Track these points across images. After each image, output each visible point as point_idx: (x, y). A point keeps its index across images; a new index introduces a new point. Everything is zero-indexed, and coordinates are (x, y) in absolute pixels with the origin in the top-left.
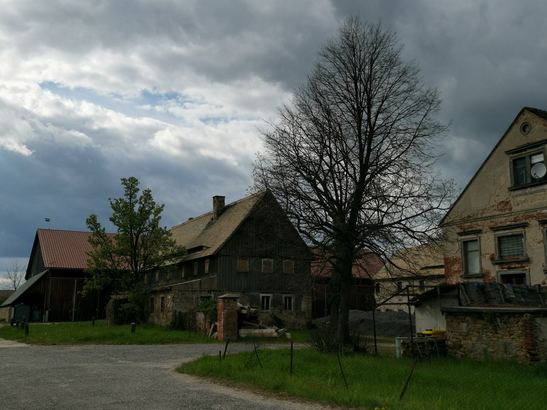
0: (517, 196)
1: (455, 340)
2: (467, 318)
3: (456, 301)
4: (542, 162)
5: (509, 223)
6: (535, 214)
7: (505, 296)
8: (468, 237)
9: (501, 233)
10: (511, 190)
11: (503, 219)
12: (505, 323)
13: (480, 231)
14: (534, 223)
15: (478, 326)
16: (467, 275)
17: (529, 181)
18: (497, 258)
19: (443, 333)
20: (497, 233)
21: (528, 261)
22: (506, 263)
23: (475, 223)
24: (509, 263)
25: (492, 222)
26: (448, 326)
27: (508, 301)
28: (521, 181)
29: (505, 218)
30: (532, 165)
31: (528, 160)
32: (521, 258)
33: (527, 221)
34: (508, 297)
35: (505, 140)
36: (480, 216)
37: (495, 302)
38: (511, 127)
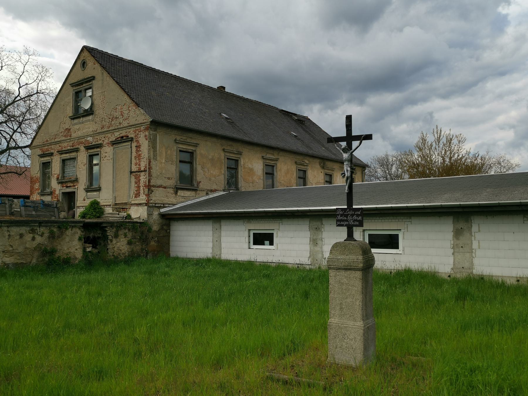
0: (76, 124)
5: (69, 148)
8: (45, 159)
9: (65, 156)
10: (73, 118)
11: (66, 144)
13: (52, 154)
14: (82, 148)
23: (50, 147)
24: (67, 182)
25: (60, 146)
29: (67, 144)
32: (73, 179)
33: (79, 147)
35: (72, 74)
36: (53, 141)
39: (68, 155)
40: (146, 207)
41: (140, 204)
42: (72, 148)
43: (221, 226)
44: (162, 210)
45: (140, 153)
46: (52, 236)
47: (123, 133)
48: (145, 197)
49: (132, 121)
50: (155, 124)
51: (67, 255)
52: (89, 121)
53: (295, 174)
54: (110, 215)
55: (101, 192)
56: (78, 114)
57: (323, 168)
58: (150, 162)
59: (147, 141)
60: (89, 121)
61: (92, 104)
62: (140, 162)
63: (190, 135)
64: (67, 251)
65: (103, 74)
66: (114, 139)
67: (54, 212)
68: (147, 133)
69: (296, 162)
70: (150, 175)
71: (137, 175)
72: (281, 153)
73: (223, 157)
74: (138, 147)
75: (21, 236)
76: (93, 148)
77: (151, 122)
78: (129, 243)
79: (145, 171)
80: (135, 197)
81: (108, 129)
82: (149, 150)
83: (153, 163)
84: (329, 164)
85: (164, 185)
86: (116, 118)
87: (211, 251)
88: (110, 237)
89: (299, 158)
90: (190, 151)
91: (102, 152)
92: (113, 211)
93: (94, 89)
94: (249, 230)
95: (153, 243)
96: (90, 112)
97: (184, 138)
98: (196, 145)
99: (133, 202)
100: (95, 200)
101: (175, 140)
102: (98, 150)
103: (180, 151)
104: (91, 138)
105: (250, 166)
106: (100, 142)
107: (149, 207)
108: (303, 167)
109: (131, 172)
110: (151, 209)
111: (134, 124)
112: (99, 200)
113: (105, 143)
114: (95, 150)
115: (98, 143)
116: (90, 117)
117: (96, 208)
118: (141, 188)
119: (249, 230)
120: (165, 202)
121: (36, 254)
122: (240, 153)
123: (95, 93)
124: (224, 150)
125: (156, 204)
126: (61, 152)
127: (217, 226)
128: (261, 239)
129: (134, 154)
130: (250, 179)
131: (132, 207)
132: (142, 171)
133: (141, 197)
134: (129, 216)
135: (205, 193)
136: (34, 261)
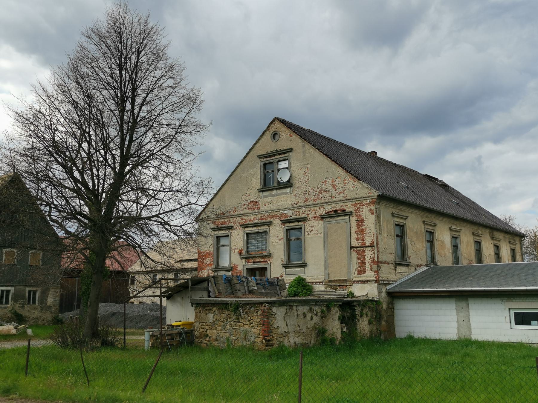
0: (265, 197)
1: (202, 330)
2: (214, 309)
3: (205, 293)
4: (286, 168)
5: (256, 221)
6: (278, 214)
7: (248, 288)
8: (220, 232)
9: (249, 230)
10: (260, 191)
11: (252, 217)
12: (246, 313)
13: (231, 228)
14: (277, 222)
15: (224, 316)
16: (218, 269)
17: (275, 184)
18: (244, 252)
19: (191, 324)
20: (246, 229)
21: (270, 256)
22: (252, 258)
23: (228, 219)
24: (254, 257)
25: (242, 219)
26: (196, 316)
27: (251, 292)
28: (269, 184)
29: (254, 217)
30: (279, 170)
31: (275, 165)
32: (265, 253)
33: (272, 220)
34: (251, 289)
35: (258, 145)
36: (232, 213)
37: (239, 294)
38: (263, 133)
39: (254, 228)
40: (376, 284)
41: (367, 281)
42: (260, 221)
43: (468, 304)
44: (388, 287)
45: (363, 227)
46: (323, 316)
47: (338, 207)
48: (373, 273)
49: (351, 195)
50: (382, 198)
51: (332, 335)
52: (286, 193)
53: (473, 246)
54: (323, 293)
55: (306, 269)
56: (269, 184)
57: (492, 238)
58: (377, 237)
59: (374, 216)
60: (286, 193)
61: (291, 176)
62: (363, 237)
63: (401, 207)
64: (331, 332)
65: (304, 146)
66: (324, 213)
67: (276, 289)
68: (372, 207)
69: (473, 233)
70: (378, 251)
71: (360, 250)
72: (462, 224)
73: (423, 230)
74: (360, 222)
75: (305, 315)
76: (294, 222)
77: (379, 196)
78: (370, 323)
79: (372, 246)
80: (358, 273)
81: (314, 203)
82: (376, 224)
83: (379, 238)
84: (497, 234)
85: (388, 261)
86: (326, 191)
87: (456, 331)
88: (358, 317)
89: (475, 228)
90: (402, 224)
91: (307, 226)
92: (326, 288)
93: (292, 161)
94: (509, 309)
95: (384, 323)
96: (289, 184)
97: (397, 211)
98: (405, 218)
99: (355, 279)
100: (299, 277)
101: (393, 213)
102: (300, 223)
103: (396, 225)
104: (290, 211)
105: (442, 238)
106: (303, 216)
107: (379, 284)
108: (478, 238)
109: (352, 248)
110: (381, 286)
111: (352, 197)
112: (304, 277)
113: (310, 216)
114: (296, 224)
115: (300, 217)
116: (288, 190)
117: (301, 285)
118: (367, 265)
119: (509, 309)
120: (389, 279)
121: (314, 334)
122: (435, 225)
123: (292, 165)
124: (424, 222)
125: (384, 281)
126: (244, 226)
127: (463, 304)
128: (522, 319)
129: (354, 228)
130: (443, 252)
131: (354, 285)
132: (366, 247)
133: (367, 273)
134: (351, 294)
135: (414, 268)
136: (312, 342)
